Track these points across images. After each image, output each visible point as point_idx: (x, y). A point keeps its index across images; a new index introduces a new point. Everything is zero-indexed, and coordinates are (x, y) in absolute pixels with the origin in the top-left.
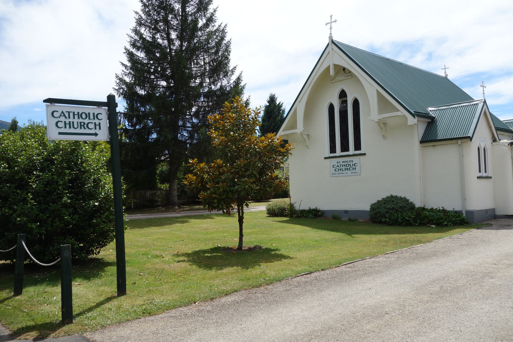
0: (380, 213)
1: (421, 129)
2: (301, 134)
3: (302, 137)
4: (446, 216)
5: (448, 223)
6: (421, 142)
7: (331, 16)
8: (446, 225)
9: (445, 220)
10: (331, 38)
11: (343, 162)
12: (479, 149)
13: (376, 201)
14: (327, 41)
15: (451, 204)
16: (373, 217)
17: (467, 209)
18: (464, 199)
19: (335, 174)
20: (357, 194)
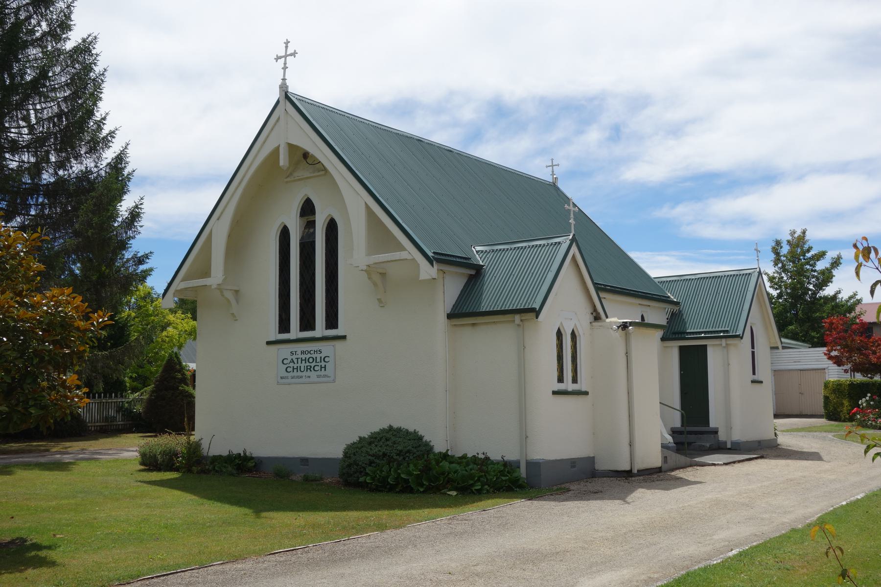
0: (358, 465)
1: (451, 288)
2: (220, 288)
3: (223, 295)
4: (482, 471)
5: (483, 486)
6: (450, 316)
7: (287, 43)
8: (479, 492)
9: (479, 480)
10: (284, 88)
11: (303, 352)
12: (559, 334)
13: (355, 439)
14: (275, 95)
15: (498, 446)
16: (344, 474)
17: (529, 458)
18: (524, 438)
19: (287, 378)
20: (319, 424)
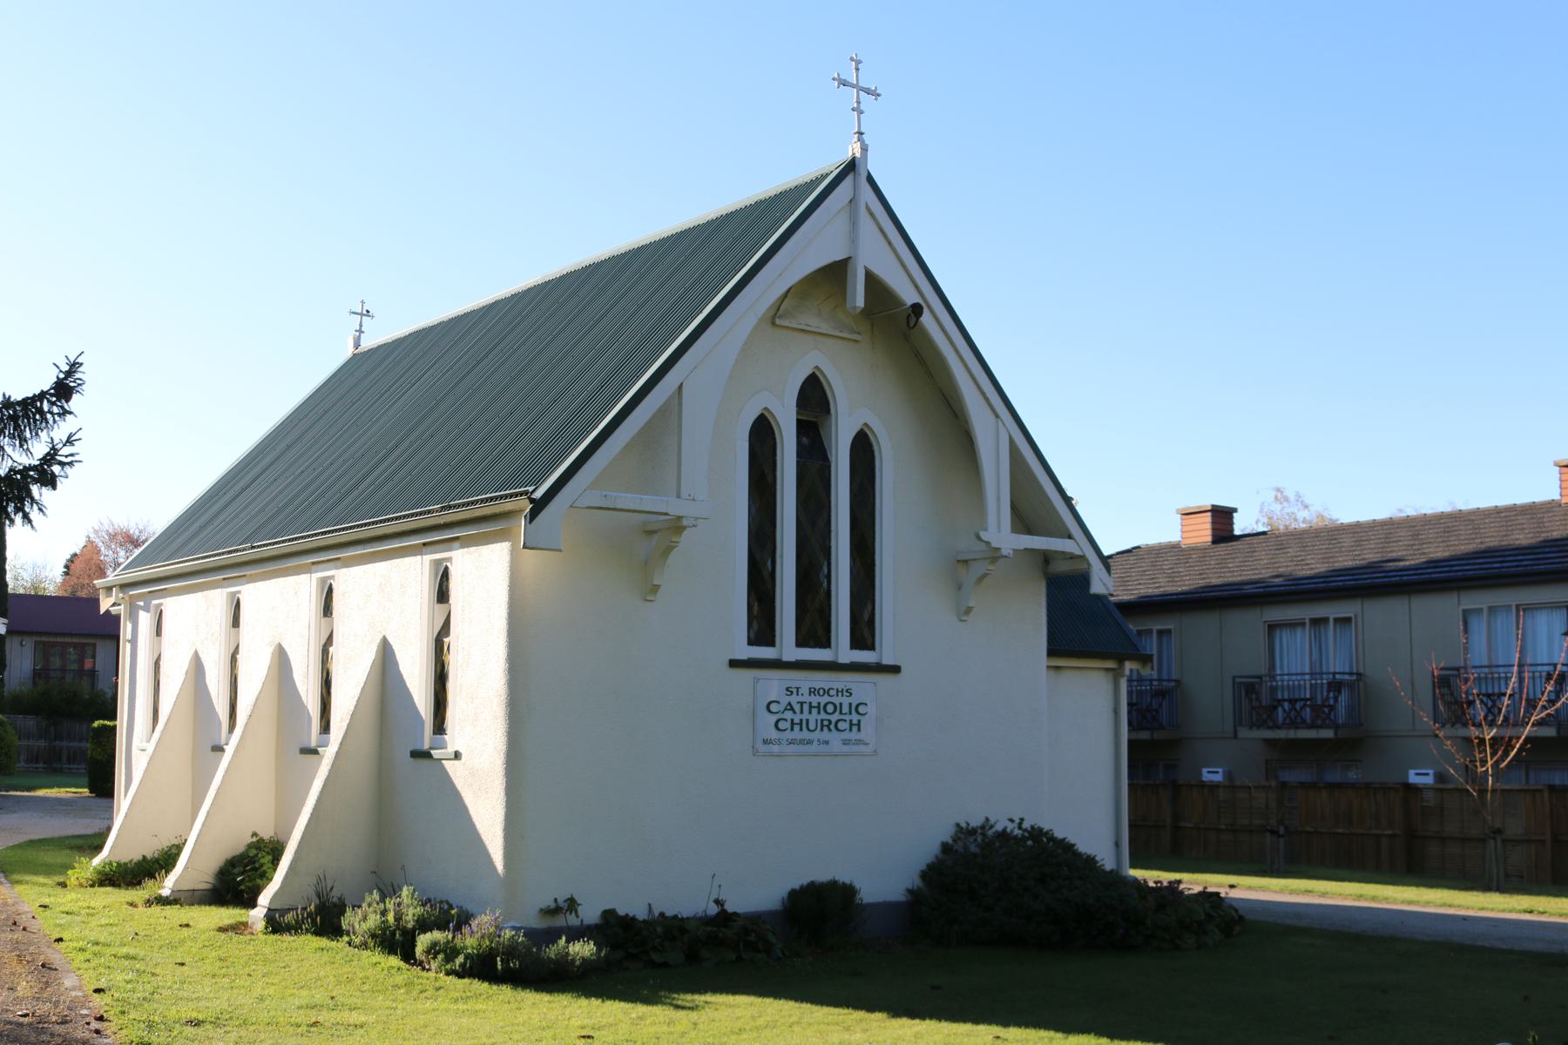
11: (812, 691)
